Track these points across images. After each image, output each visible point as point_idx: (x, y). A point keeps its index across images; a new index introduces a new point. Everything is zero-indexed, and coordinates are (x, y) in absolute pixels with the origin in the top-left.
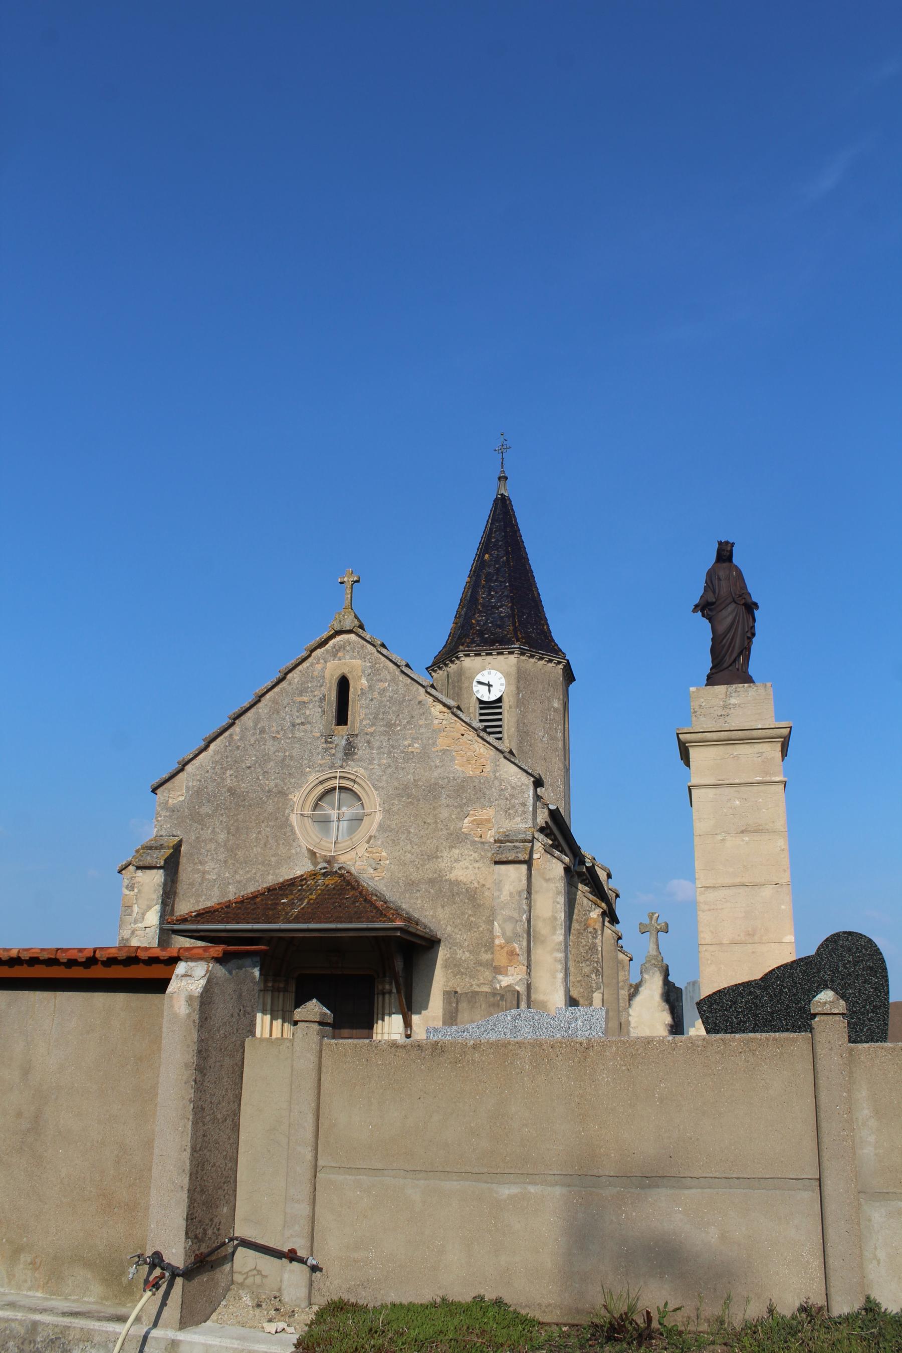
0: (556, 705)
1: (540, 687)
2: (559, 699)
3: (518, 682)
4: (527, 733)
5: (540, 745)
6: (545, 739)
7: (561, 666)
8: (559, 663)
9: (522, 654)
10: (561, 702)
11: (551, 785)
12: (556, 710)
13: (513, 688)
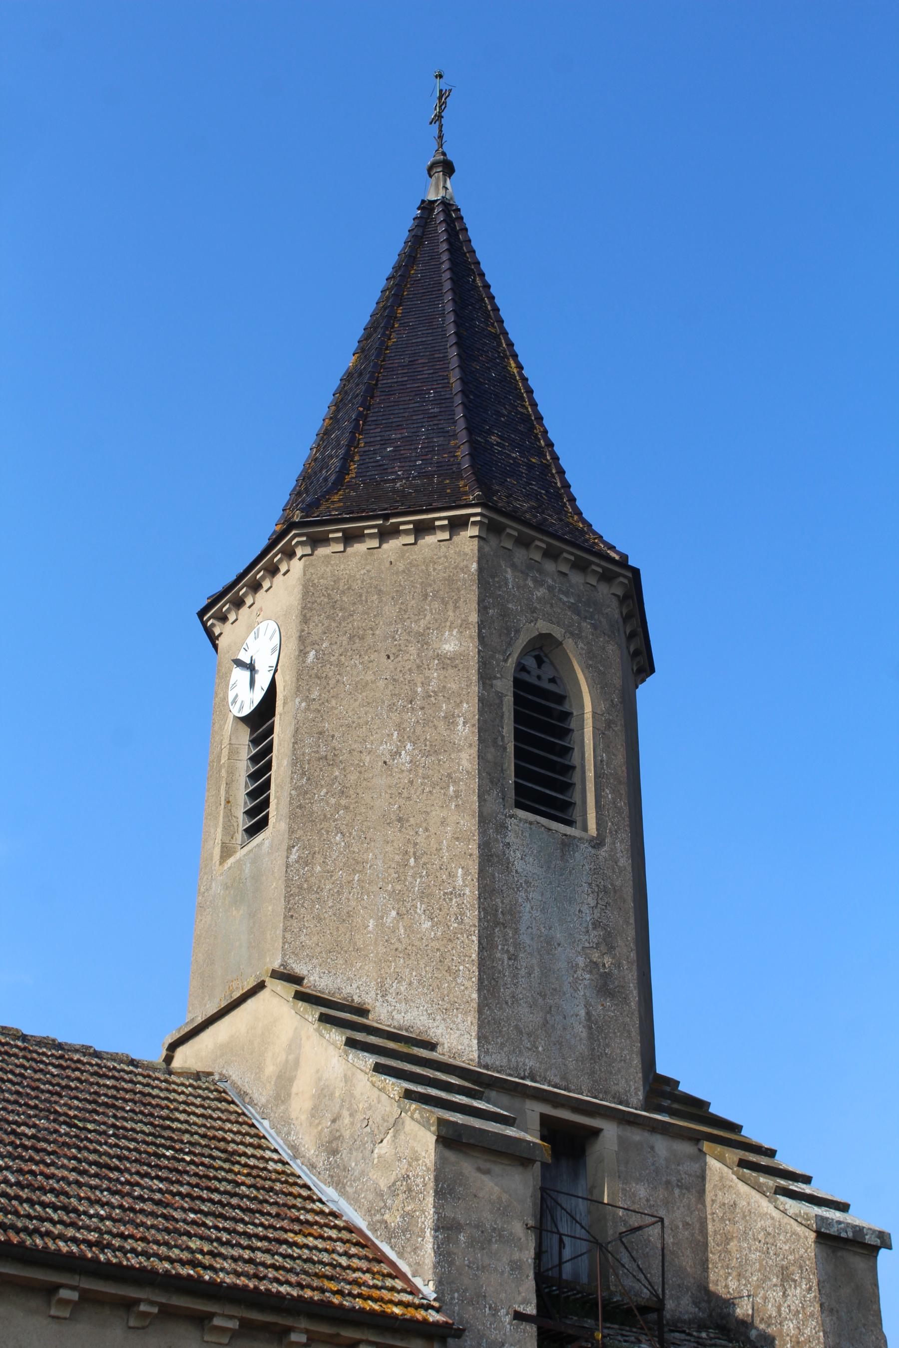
0: (450, 647)
1: (390, 610)
2: (464, 625)
3: (305, 620)
4: (330, 760)
5: (382, 782)
6: (405, 757)
7: (473, 531)
8: (457, 525)
9: (316, 541)
10: (474, 631)
11: (424, 895)
12: (447, 662)
13: (291, 646)
